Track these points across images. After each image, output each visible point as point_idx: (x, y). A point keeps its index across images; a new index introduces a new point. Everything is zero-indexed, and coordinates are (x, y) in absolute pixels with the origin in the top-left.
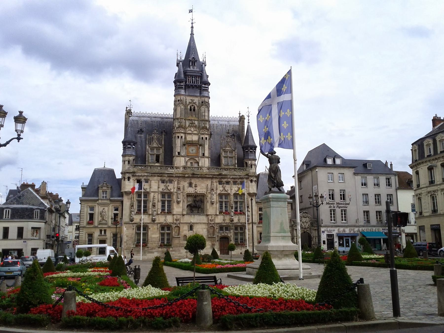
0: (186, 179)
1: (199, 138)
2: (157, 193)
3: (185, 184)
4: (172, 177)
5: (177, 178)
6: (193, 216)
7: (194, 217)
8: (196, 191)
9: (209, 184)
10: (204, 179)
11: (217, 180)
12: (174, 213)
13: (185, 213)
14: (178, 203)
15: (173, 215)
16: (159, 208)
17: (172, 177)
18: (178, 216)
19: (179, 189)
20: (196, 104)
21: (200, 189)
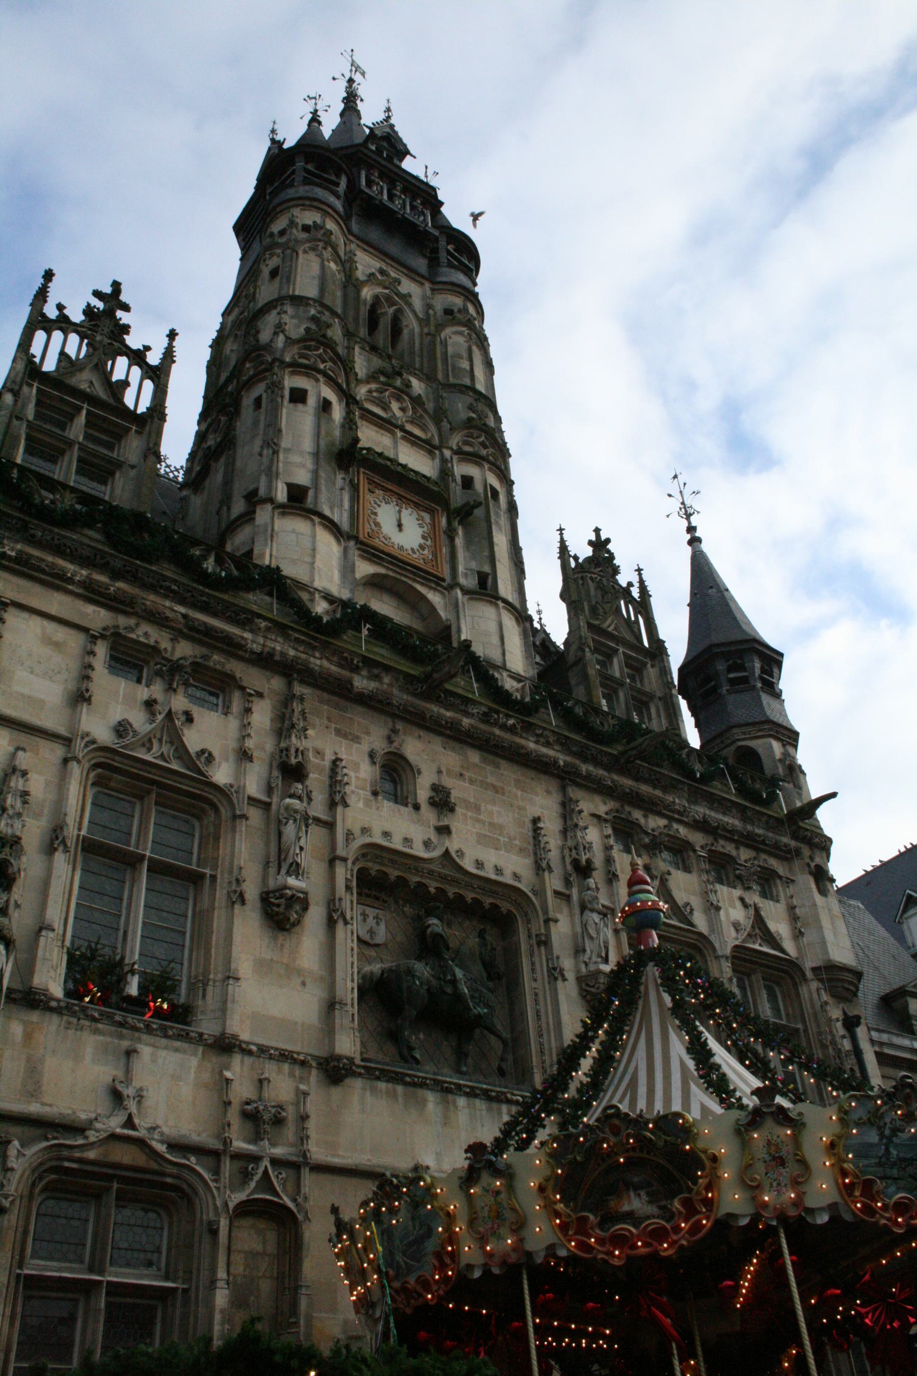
0: (360, 718)
1: (445, 473)
2: (53, 753)
3: (344, 748)
4: (233, 648)
5: (277, 683)
6: (431, 1098)
7: (446, 1121)
8: (453, 844)
9: (551, 826)
10: (509, 773)
11: (602, 807)
12: (240, 1027)
13: (347, 1044)
14: (281, 913)
15: (225, 1046)
16: (54, 914)
17: (233, 648)
18: (270, 1069)
19: (292, 771)
20: (410, 305)
21: (482, 839)
